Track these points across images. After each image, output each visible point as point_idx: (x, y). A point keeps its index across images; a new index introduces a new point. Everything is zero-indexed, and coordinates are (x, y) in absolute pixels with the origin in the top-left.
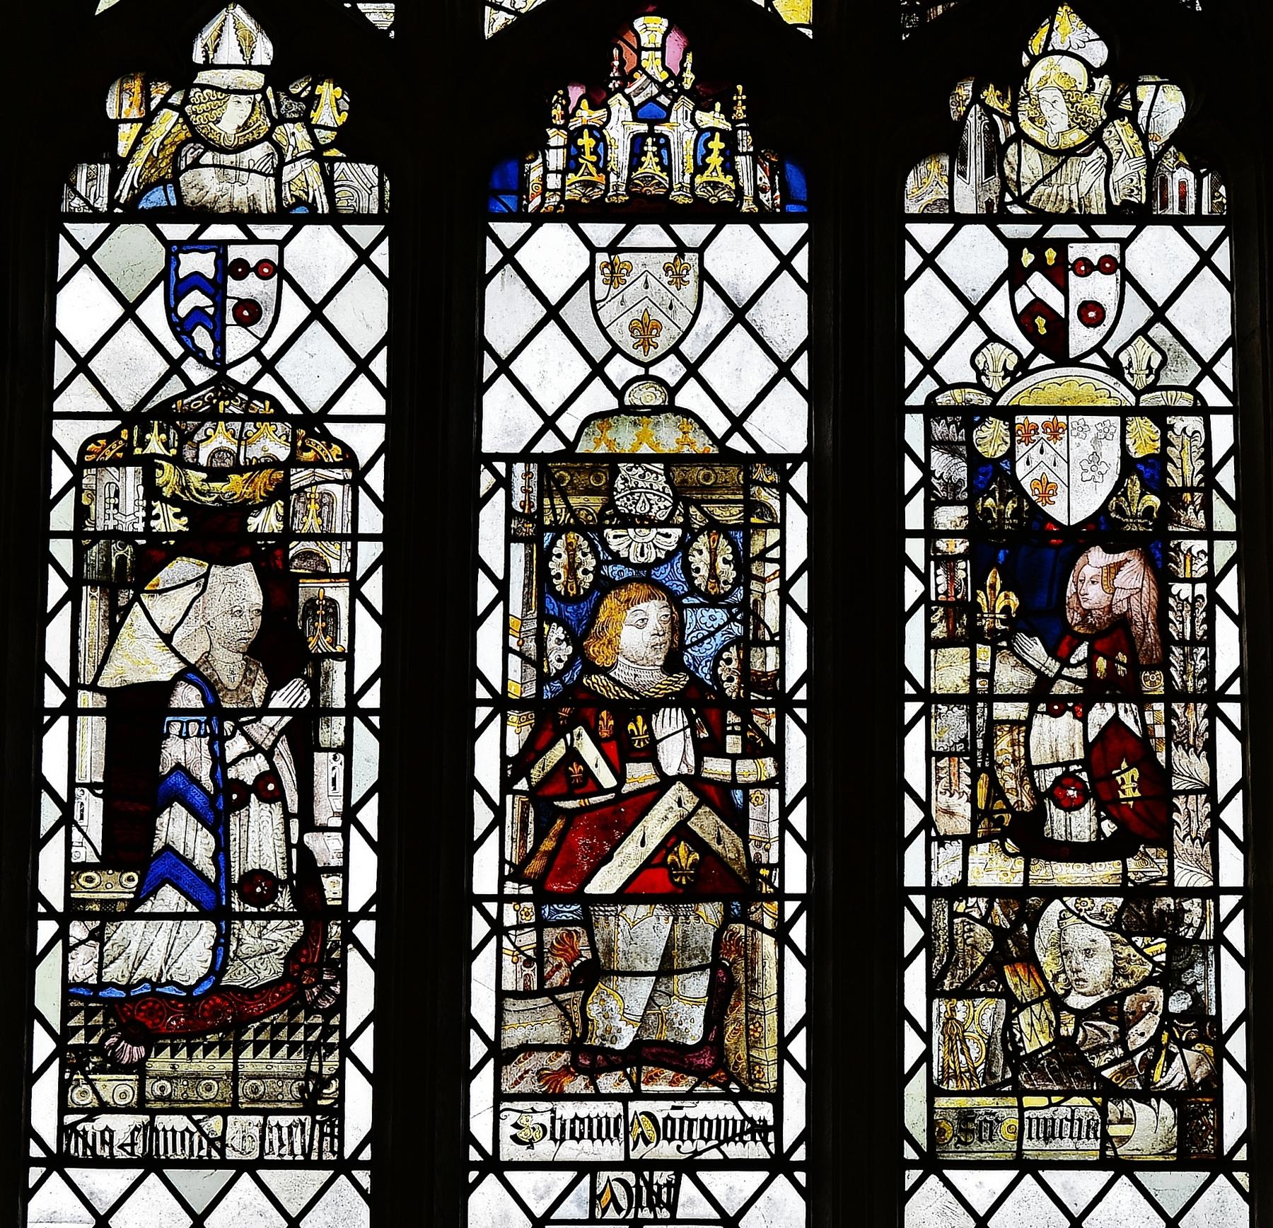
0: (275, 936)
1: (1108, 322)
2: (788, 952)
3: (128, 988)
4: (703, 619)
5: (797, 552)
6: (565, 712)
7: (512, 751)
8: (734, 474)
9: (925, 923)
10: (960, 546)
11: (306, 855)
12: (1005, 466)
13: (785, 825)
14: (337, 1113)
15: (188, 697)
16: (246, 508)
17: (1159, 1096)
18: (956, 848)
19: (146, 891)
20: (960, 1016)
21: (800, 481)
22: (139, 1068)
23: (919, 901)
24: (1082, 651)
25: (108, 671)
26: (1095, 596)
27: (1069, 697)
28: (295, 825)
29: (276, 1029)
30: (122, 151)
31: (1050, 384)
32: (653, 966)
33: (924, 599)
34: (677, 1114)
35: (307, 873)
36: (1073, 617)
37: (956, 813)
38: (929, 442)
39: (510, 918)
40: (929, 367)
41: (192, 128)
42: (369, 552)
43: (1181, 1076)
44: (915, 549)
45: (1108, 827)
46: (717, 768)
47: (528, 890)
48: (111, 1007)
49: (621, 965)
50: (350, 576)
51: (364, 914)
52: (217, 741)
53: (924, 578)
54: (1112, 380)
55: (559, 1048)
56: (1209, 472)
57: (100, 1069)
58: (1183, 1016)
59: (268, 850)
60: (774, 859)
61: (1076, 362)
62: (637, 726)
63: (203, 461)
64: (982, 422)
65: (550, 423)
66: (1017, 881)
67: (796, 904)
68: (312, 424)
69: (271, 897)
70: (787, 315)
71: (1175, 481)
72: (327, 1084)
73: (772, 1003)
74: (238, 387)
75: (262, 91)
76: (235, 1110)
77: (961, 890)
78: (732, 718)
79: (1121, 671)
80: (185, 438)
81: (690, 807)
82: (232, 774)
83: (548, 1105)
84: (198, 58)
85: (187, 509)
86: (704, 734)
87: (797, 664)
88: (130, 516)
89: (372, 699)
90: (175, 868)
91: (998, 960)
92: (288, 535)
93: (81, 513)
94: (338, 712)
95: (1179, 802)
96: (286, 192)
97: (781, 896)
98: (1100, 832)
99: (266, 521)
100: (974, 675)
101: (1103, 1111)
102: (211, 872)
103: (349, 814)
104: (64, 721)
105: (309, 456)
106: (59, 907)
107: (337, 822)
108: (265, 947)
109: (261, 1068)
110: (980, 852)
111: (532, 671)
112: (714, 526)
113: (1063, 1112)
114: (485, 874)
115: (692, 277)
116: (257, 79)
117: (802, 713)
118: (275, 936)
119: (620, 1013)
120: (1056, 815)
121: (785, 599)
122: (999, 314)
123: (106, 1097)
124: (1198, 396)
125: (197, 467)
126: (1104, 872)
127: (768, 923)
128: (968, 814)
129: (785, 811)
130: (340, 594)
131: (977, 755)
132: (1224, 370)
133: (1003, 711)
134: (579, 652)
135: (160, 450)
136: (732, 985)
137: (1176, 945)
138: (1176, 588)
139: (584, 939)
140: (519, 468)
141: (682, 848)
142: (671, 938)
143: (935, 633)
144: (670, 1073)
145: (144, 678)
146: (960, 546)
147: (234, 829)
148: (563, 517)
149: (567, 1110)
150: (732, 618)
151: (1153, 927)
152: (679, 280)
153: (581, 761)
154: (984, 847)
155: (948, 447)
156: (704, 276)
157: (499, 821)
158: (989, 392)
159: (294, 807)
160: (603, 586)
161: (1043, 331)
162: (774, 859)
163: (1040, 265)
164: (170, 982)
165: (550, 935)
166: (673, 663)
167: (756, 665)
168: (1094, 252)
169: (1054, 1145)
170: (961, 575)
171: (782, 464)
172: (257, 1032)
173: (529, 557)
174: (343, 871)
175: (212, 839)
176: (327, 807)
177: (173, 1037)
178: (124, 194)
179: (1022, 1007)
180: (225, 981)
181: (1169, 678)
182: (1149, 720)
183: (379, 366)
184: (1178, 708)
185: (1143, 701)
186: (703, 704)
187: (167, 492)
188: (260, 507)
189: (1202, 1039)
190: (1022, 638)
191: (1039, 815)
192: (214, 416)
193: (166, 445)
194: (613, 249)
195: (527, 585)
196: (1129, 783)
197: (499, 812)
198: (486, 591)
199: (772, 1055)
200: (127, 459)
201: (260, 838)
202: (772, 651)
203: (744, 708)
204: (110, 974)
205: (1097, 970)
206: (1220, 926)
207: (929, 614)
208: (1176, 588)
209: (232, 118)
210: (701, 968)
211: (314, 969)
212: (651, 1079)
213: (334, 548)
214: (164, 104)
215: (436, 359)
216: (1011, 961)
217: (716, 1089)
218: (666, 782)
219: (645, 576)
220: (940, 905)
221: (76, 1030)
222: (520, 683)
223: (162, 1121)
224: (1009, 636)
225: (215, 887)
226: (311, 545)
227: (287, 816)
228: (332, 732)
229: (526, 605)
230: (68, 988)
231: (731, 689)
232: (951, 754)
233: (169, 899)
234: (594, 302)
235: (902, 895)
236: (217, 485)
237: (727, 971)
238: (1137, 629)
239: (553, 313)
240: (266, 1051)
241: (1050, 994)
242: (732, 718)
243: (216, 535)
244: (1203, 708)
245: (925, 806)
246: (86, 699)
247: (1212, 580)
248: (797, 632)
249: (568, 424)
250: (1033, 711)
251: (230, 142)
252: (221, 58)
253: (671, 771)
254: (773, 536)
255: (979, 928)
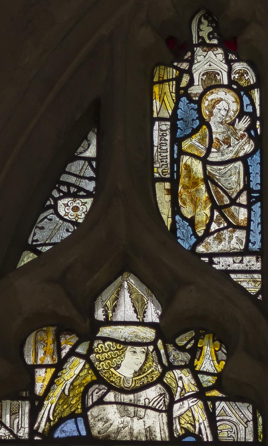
30: (39, 389)
41: (96, 372)
75: (154, 343)
84: (100, 315)
96: (177, 425)
116: (149, 334)
178: (42, 425)
209: (129, 365)
214: (72, 353)
251: (130, 384)
252: (120, 316)
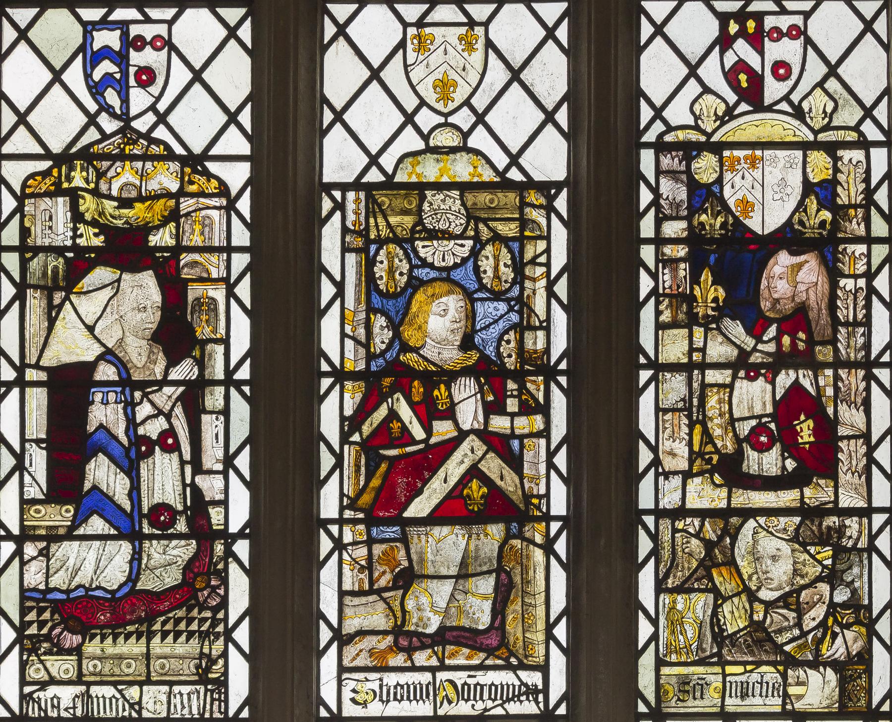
0: (175, 552)
1: (794, 77)
2: (553, 561)
3: (68, 592)
4: (488, 310)
5: (559, 259)
6: (387, 381)
7: (348, 412)
8: (512, 197)
9: (654, 537)
10: (681, 251)
11: (197, 492)
12: (716, 189)
13: (551, 465)
14: (222, 683)
15: (107, 372)
16: (147, 229)
17: (825, 665)
18: (677, 481)
19: (79, 519)
20: (679, 607)
21: (561, 203)
22: (77, 651)
23: (649, 520)
24: (772, 331)
25: (47, 354)
26: (782, 288)
27: (762, 365)
28: (188, 469)
29: (178, 621)
31: (750, 126)
32: (454, 571)
33: (654, 292)
34: (470, 681)
35: (198, 505)
36: (765, 305)
37: (677, 453)
38: (659, 172)
39: (348, 538)
40: (658, 113)
42: (240, 261)
43: (842, 650)
44: (647, 253)
45: (790, 465)
46: (500, 423)
47: (361, 516)
48: (57, 607)
49: (430, 571)
50: (226, 280)
51: (241, 535)
52: (130, 406)
53: (654, 276)
54: (797, 123)
55: (385, 633)
56: (869, 193)
57: (49, 652)
58: (844, 605)
59: (169, 488)
60: (543, 491)
61: (770, 109)
62: (440, 392)
63: (115, 193)
64: (698, 155)
65: (374, 160)
66: (723, 504)
67: (559, 524)
68: (194, 162)
69: (172, 523)
70: (552, 74)
71: (843, 198)
72: (215, 662)
73: (541, 599)
74: (140, 135)
76: (148, 682)
77: (681, 512)
78: (511, 385)
79: (801, 346)
80: (100, 175)
81: (480, 453)
82: (141, 431)
83: (376, 675)
85: (104, 229)
86: (490, 398)
87: (560, 343)
88: (62, 235)
89: (244, 373)
90: (100, 502)
91: (707, 564)
92: (178, 249)
93: (25, 232)
94: (218, 383)
95: (843, 444)
97: (547, 518)
98: (784, 468)
99: (162, 238)
100: (691, 350)
101: (784, 676)
102: (127, 506)
103: (229, 461)
104: (16, 391)
105: (193, 188)
106: (16, 531)
107: (219, 467)
108: (168, 561)
109: (167, 650)
110: (694, 484)
111: (362, 351)
112: (497, 238)
113: (755, 677)
114: (329, 503)
115: (480, 45)
117: (563, 380)
118: (175, 552)
119: (429, 606)
120: (752, 455)
121: (551, 294)
122: (712, 72)
123: (54, 673)
124: (861, 134)
125: (110, 197)
126: (788, 498)
127: (539, 539)
128: (686, 455)
129: (551, 455)
130: (219, 294)
131: (693, 410)
132: (881, 113)
133: (712, 376)
134: (397, 335)
135: (83, 184)
136: (511, 585)
137: (839, 551)
138: (842, 282)
139: (403, 553)
140: (351, 195)
141: (475, 484)
142: (466, 550)
143: (662, 318)
144: (466, 651)
145: (74, 359)
146: (681, 251)
147: (144, 473)
148: (384, 232)
149: (391, 679)
150: (511, 309)
151: (823, 540)
152: (470, 47)
153: (399, 420)
154: (698, 480)
155: (672, 174)
156: (489, 44)
157: (339, 464)
158: (703, 132)
159: (187, 456)
160: (415, 284)
161: (744, 85)
162: (543, 491)
163: (743, 33)
164: (99, 588)
165: (378, 549)
166: (467, 343)
167: (529, 344)
168: (784, 23)
169: (747, 702)
170: (682, 273)
171: (548, 189)
172: (164, 623)
173: (359, 264)
174: (224, 503)
175: (127, 481)
176: (212, 456)
177: (102, 628)
179: (725, 599)
180: (139, 586)
181: (836, 351)
182: (822, 383)
183: (245, 119)
184: (843, 373)
185: (817, 367)
186: (489, 374)
187: (88, 217)
188: (157, 228)
189: (858, 622)
190: (727, 322)
191: (739, 455)
192: (122, 157)
193: (87, 181)
194: (420, 23)
195: (358, 285)
196: (806, 431)
197: (339, 459)
198: (327, 290)
199: (541, 637)
200: (58, 191)
201: (163, 479)
202: (541, 334)
203: (519, 376)
204: (54, 582)
205: (781, 572)
206: (872, 538)
207: (658, 303)
208: (842, 282)
210: (489, 572)
211: (203, 574)
212: (453, 655)
213: (214, 258)
215: (287, 112)
216: (718, 565)
217: (500, 662)
218: (463, 435)
219: (446, 276)
220: (665, 524)
221: (31, 623)
222: (354, 360)
223: (95, 690)
224: (717, 320)
225: (130, 516)
226: (196, 257)
227: (183, 463)
228: (214, 398)
229: (358, 301)
230: (24, 593)
231: (511, 363)
232: (673, 410)
233: (97, 525)
234: (406, 66)
235: (635, 516)
236: (125, 211)
237: (508, 574)
238: (812, 315)
239: (375, 74)
240: (170, 637)
241: (747, 590)
242: (511, 385)
243: (126, 249)
244: (861, 373)
245: (654, 449)
246: (31, 375)
247: (870, 276)
248: (560, 319)
249: (388, 161)
250: (735, 377)
253: (466, 427)
254: (541, 245)
255: (694, 542)
